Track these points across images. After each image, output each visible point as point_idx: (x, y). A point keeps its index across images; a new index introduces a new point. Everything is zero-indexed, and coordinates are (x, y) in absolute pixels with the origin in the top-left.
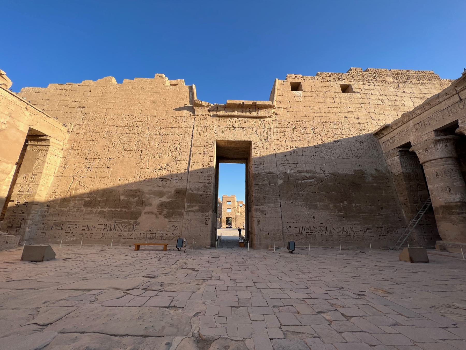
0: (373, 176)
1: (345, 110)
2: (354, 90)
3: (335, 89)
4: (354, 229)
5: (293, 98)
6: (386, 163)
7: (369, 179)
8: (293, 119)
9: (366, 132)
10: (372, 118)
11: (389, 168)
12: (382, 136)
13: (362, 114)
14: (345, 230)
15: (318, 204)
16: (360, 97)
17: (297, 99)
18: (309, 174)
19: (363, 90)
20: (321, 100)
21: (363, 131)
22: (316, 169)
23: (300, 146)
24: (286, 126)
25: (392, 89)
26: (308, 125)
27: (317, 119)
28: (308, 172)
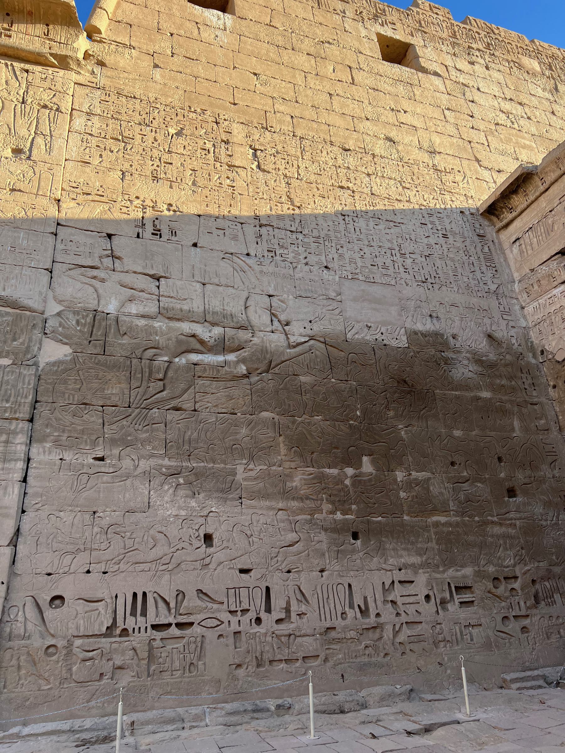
0: (479, 361)
1: (391, 117)
2: (423, 63)
3: (360, 42)
4: (397, 593)
5: (190, 26)
6: (525, 317)
7: (464, 370)
8: (176, 98)
9: (459, 203)
10: (478, 161)
11: (533, 336)
12: (510, 216)
13: (447, 140)
14: (358, 600)
15: (240, 469)
16: (442, 88)
17: (206, 35)
18: (217, 331)
19: (453, 72)
20: (302, 61)
21: (447, 197)
22: (251, 310)
23: (192, 209)
24: (138, 118)
25: (540, 92)
26: (238, 133)
27: (280, 122)
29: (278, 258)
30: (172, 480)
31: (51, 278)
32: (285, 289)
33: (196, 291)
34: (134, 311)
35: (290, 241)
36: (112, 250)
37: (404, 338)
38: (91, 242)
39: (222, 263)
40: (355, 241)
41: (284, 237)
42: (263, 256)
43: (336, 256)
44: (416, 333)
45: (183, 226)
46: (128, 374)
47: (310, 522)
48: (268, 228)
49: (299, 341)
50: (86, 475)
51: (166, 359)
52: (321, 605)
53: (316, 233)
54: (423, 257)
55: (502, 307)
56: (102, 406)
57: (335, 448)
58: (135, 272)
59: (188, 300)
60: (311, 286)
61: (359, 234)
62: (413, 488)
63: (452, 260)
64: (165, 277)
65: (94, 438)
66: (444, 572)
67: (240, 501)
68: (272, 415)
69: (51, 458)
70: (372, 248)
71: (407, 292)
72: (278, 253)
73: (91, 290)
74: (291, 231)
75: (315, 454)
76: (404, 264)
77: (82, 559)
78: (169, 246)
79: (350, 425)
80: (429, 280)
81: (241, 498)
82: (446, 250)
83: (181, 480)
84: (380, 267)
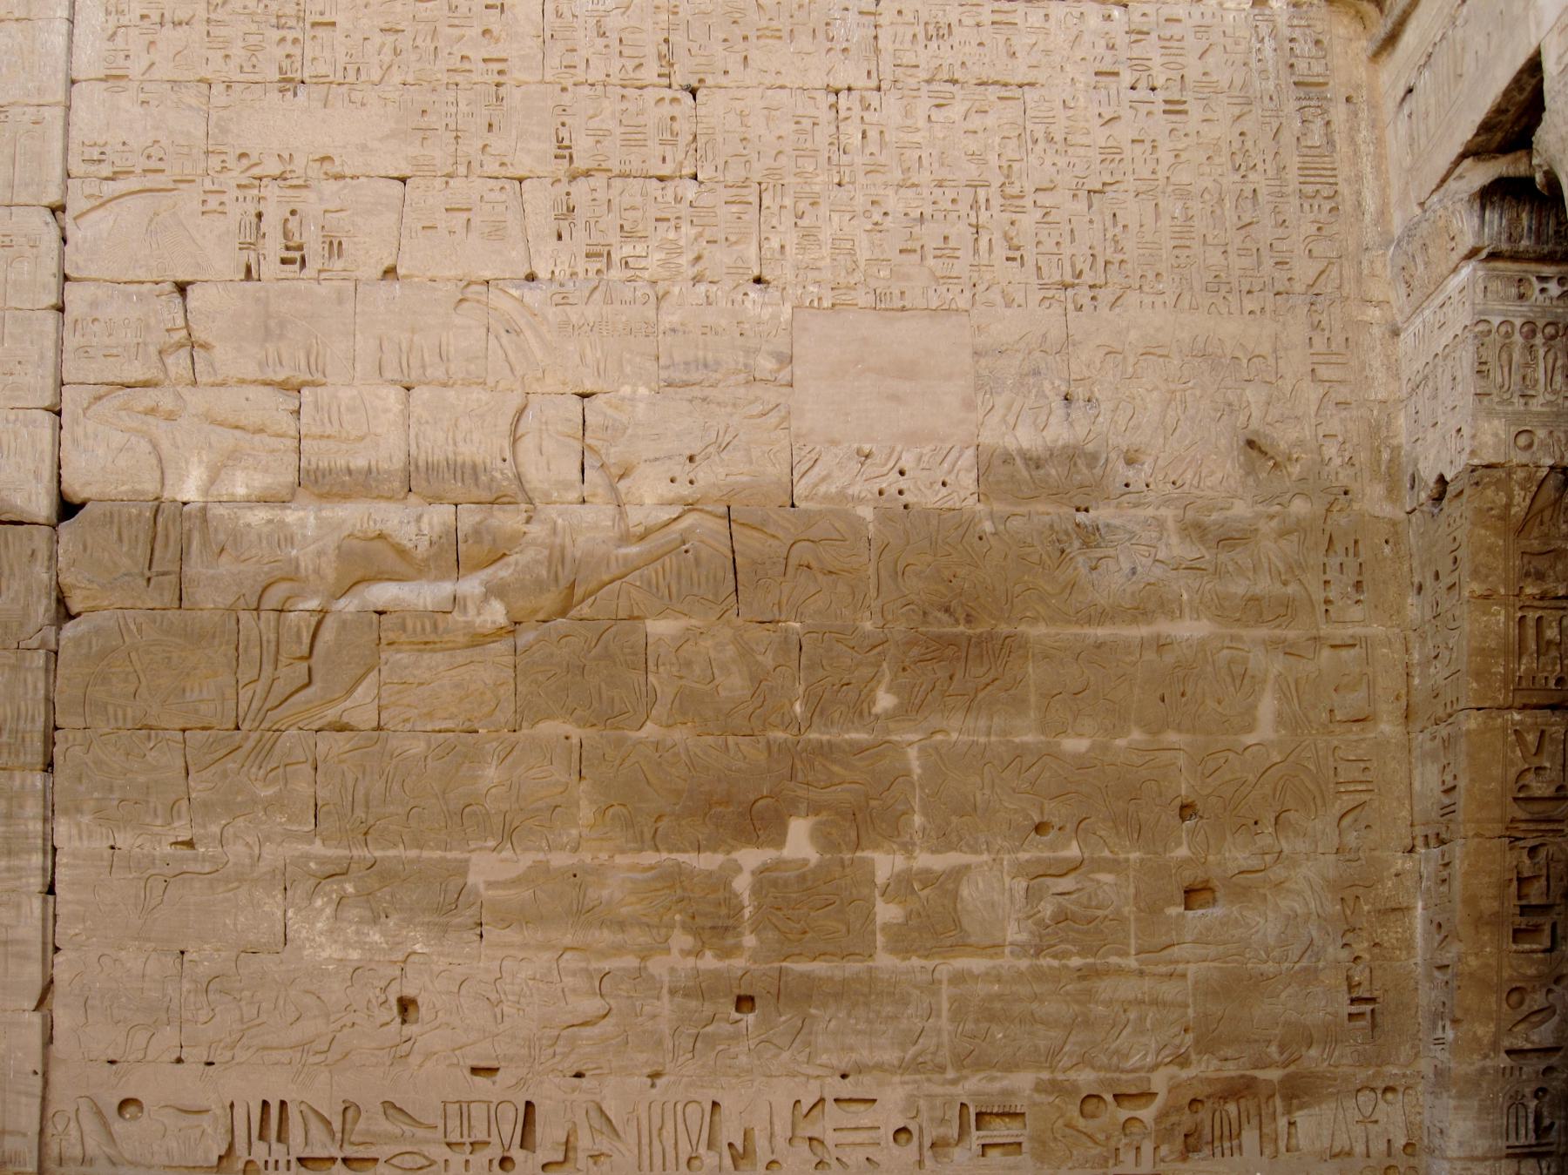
4: (826, 1125)
22: (527, 444)
28: (413, 481)
32: (628, 370)
33: (386, 411)
34: (241, 491)
35: (653, 212)
36: (187, 326)
37: (968, 480)
42: (573, 274)
43: (792, 239)
44: (1007, 459)
46: (232, 652)
51: (313, 604)
52: (645, 1140)
54: (1083, 194)
55: (1319, 344)
58: (242, 382)
59: (368, 440)
61: (874, 149)
62: (913, 891)
63: (1183, 193)
64: (313, 384)
66: (954, 1082)
72: (615, 257)
74: (661, 179)
75: (666, 819)
77: (168, 1037)
78: (324, 290)
80: (1088, 278)
84: (929, 253)
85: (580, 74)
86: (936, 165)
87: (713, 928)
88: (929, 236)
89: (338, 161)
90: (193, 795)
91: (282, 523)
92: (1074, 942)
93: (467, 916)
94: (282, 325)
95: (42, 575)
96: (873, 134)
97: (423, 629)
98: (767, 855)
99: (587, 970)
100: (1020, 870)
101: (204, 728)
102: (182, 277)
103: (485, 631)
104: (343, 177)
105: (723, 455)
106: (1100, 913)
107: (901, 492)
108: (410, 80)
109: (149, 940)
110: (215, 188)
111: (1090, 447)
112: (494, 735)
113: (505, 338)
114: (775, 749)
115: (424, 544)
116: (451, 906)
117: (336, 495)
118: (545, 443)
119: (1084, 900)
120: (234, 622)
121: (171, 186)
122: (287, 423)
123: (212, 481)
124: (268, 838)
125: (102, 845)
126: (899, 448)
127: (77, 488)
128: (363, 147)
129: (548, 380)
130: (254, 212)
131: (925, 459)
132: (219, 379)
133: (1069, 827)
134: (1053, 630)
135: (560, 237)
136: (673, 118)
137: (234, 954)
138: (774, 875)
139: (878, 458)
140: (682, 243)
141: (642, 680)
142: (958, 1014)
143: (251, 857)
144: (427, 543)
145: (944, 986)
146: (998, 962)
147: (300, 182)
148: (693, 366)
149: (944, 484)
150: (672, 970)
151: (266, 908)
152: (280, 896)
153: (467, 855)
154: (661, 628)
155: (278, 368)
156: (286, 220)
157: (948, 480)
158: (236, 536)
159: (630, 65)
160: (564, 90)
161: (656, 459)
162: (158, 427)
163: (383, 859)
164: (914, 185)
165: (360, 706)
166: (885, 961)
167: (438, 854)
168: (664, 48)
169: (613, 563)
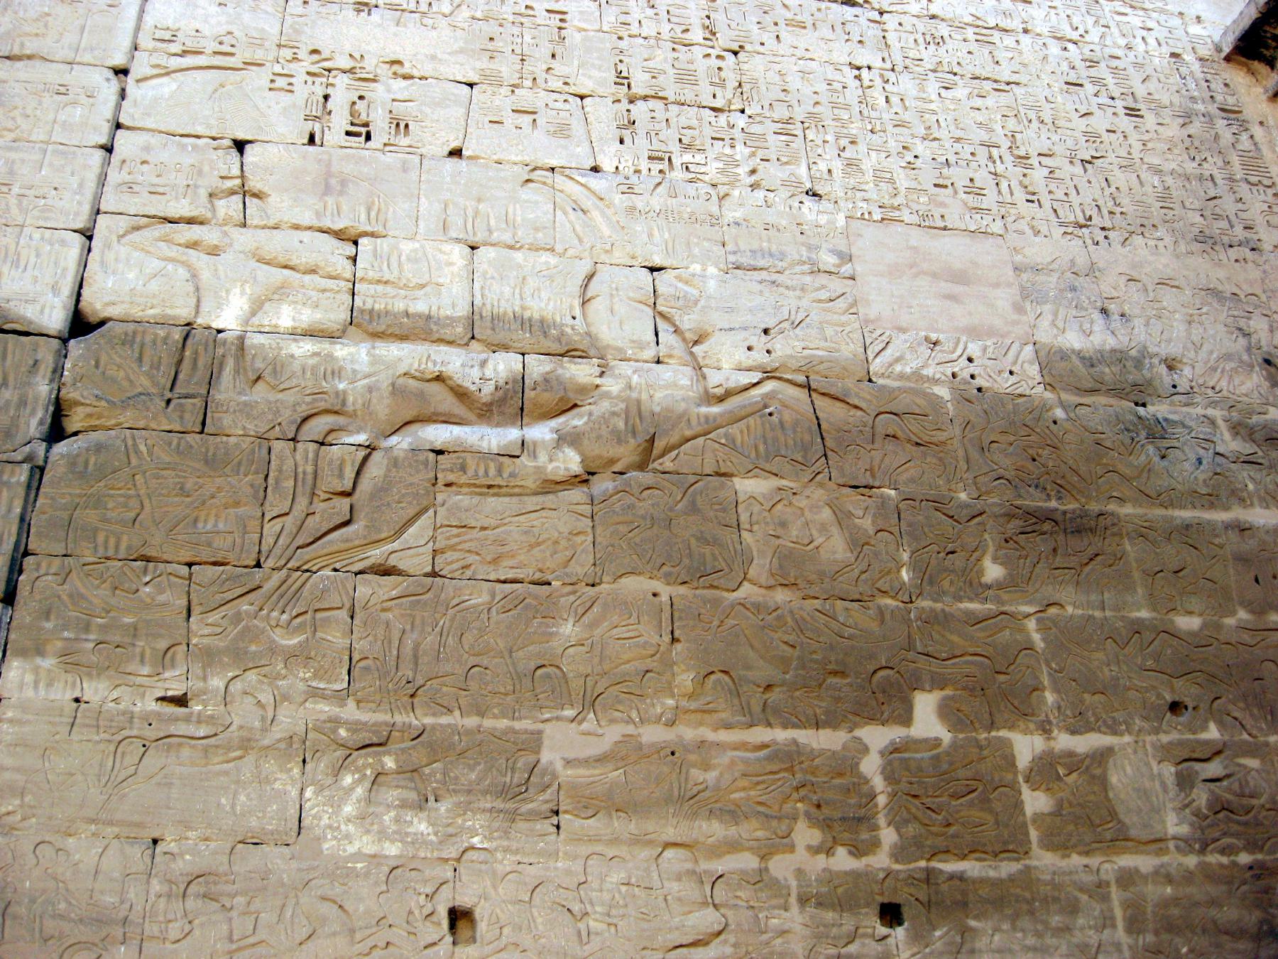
28: (477, 330)
29: (678, 175)
30: (365, 760)
31: (89, 250)
32: (696, 251)
33: (451, 264)
35: (709, 132)
36: (242, 176)
37: (1034, 370)
38: (192, 161)
39: (527, 193)
40: (890, 128)
41: (694, 123)
43: (837, 166)
44: (1064, 355)
45: (428, 111)
47: (760, 879)
48: (652, 104)
49: (731, 384)
50: (139, 743)
51: (362, 438)
53: (781, 112)
56: (190, 565)
57: (835, 673)
58: (297, 227)
59: (428, 289)
60: (769, 241)
62: (1059, 778)
64: (372, 235)
65: (162, 644)
67: (555, 820)
68: (657, 585)
69: (52, 697)
70: (935, 144)
71: (1037, 251)
72: (677, 161)
73: (182, 272)
74: (713, 109)
76: (1026, 181)
78: (389, 158)
79: (881, 611)
80: (1096, 220)
81: (557, 813)
82: (1137, 146)
83: (390, 763)
85: (634, 29)
86: (952, 128)
87: (843, 819)
88: (959, 176)
89: (407, 65)
90: (194, 641)
91: (330, 356)
92: (1236, 835)
93: (540, 802)
94: (343, 183)
95: (43, 388)
96: (895, 100)
97: (486, 472)
98: (894, 733)
99: (694, 872)
100: (1165, 752)
101: (215, 564)
102: (241, 136)
103: (558, 479)
104: (412, 77)
105: (797, 331)
106: (1254, 802)
107: (972, 377)
108: (479, 15)
109: (111, 823)
110: (285, 72)
111: (1133, 353)
112: (570, 588)
113: (572, 214)
114: (888, 617)
115: (488, 388)
116: (518, 788)
117: (391, 335)
118: (616, 307)
119: (1236, 786)
120: (265, 451)
121: (242, 66)
122: (345, 268)
123: (253, 314)
124: (286, 698)
125: (62, 694)
126: (964, 338)
127: (98, 306)
128: (433, 57)
129: (617, 253)
130: (321, 94)
131: (991, 350)
132: (271, 223)
133: (1203, 706)
134: (1140, 511)
135: (622, 142)
136: (719, 69)
137: (229, 846)
138: (906, 755)
139: (947, 346)
140: (738, 157)
141: (735, 537)
142: (1134, 925)
143: (263, 719)
144: (492, 388)
145: (1113, 889)
146: (1166, 859)
147: (371, 76)
148: (759, 254)
149: (1011, 373)
150: (800, 872)
151: (277, 785)
152: (296, 771)
153: (541, 726)
154: (747, 486)
155: (336, 219)
156: (354, 103)
157: (1013, 369)
158: (277, 366)
159: (679, 29)
160: (620, 38)
161: (731, 329)
162: (199, 259)
163: (433, 727)
164: (935, 139)
165: (413, 550)
166: (1044, 860)
167: (503, 723)
168: (707, 22)
169: (694, 422)
